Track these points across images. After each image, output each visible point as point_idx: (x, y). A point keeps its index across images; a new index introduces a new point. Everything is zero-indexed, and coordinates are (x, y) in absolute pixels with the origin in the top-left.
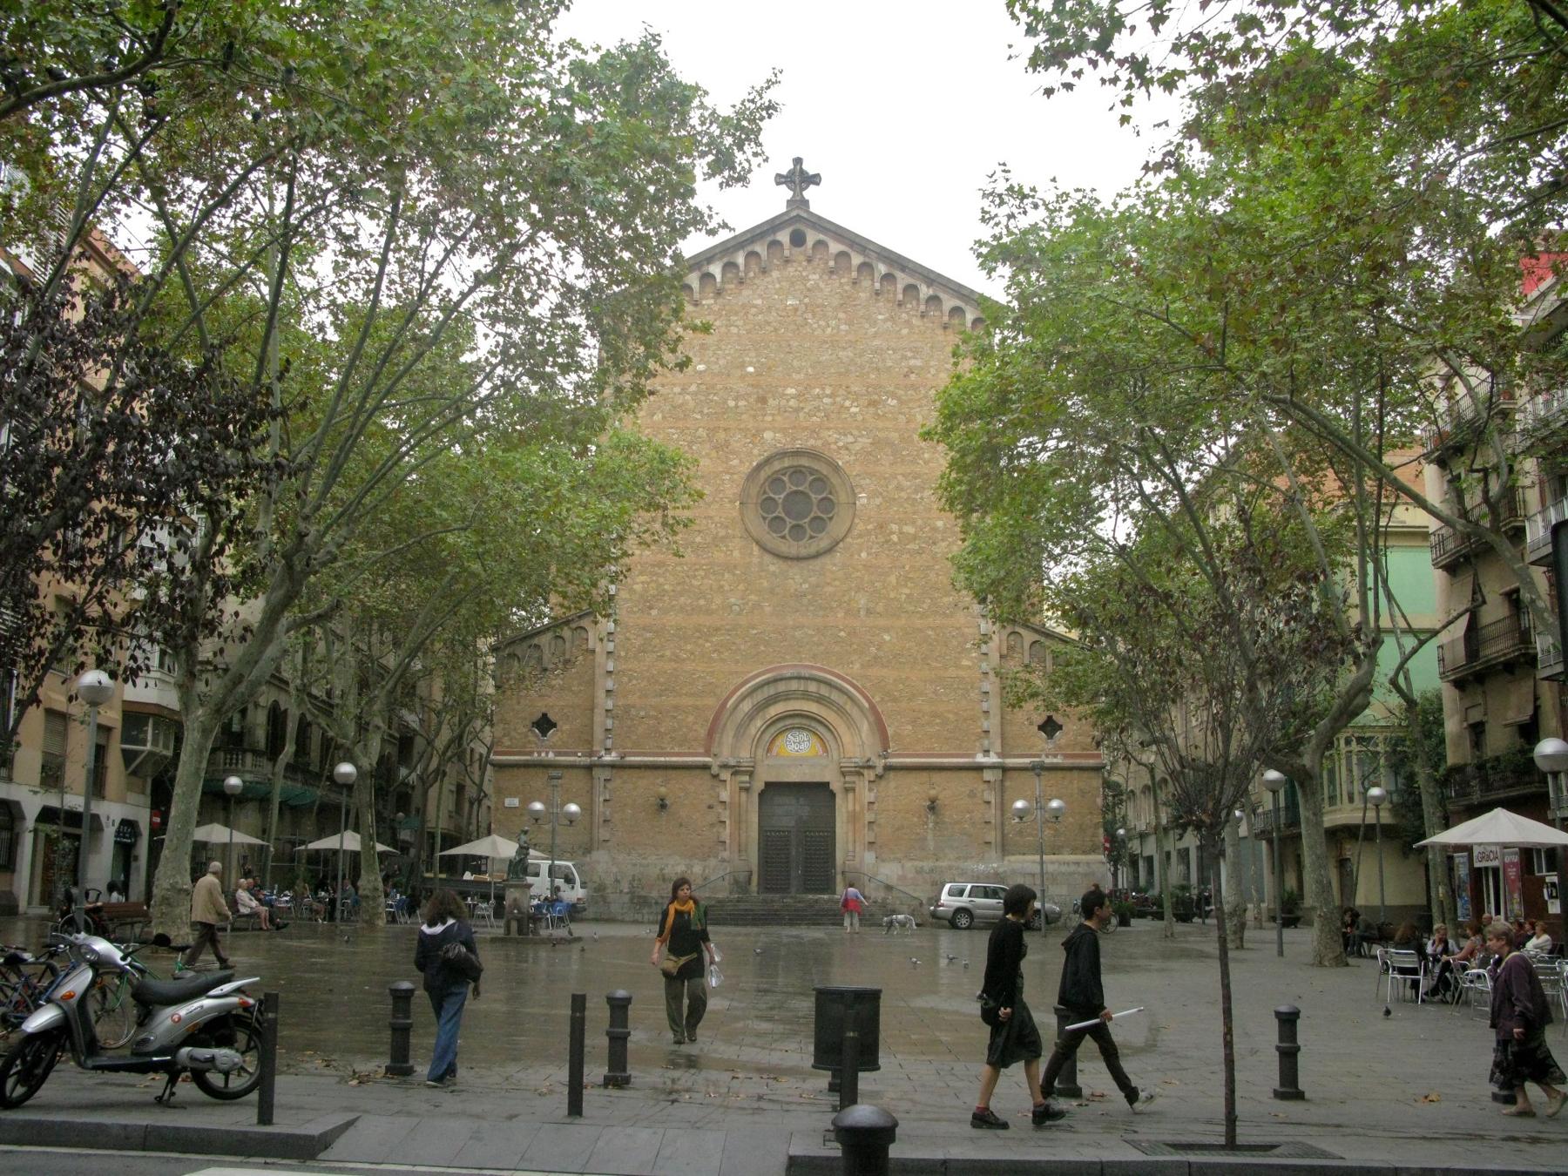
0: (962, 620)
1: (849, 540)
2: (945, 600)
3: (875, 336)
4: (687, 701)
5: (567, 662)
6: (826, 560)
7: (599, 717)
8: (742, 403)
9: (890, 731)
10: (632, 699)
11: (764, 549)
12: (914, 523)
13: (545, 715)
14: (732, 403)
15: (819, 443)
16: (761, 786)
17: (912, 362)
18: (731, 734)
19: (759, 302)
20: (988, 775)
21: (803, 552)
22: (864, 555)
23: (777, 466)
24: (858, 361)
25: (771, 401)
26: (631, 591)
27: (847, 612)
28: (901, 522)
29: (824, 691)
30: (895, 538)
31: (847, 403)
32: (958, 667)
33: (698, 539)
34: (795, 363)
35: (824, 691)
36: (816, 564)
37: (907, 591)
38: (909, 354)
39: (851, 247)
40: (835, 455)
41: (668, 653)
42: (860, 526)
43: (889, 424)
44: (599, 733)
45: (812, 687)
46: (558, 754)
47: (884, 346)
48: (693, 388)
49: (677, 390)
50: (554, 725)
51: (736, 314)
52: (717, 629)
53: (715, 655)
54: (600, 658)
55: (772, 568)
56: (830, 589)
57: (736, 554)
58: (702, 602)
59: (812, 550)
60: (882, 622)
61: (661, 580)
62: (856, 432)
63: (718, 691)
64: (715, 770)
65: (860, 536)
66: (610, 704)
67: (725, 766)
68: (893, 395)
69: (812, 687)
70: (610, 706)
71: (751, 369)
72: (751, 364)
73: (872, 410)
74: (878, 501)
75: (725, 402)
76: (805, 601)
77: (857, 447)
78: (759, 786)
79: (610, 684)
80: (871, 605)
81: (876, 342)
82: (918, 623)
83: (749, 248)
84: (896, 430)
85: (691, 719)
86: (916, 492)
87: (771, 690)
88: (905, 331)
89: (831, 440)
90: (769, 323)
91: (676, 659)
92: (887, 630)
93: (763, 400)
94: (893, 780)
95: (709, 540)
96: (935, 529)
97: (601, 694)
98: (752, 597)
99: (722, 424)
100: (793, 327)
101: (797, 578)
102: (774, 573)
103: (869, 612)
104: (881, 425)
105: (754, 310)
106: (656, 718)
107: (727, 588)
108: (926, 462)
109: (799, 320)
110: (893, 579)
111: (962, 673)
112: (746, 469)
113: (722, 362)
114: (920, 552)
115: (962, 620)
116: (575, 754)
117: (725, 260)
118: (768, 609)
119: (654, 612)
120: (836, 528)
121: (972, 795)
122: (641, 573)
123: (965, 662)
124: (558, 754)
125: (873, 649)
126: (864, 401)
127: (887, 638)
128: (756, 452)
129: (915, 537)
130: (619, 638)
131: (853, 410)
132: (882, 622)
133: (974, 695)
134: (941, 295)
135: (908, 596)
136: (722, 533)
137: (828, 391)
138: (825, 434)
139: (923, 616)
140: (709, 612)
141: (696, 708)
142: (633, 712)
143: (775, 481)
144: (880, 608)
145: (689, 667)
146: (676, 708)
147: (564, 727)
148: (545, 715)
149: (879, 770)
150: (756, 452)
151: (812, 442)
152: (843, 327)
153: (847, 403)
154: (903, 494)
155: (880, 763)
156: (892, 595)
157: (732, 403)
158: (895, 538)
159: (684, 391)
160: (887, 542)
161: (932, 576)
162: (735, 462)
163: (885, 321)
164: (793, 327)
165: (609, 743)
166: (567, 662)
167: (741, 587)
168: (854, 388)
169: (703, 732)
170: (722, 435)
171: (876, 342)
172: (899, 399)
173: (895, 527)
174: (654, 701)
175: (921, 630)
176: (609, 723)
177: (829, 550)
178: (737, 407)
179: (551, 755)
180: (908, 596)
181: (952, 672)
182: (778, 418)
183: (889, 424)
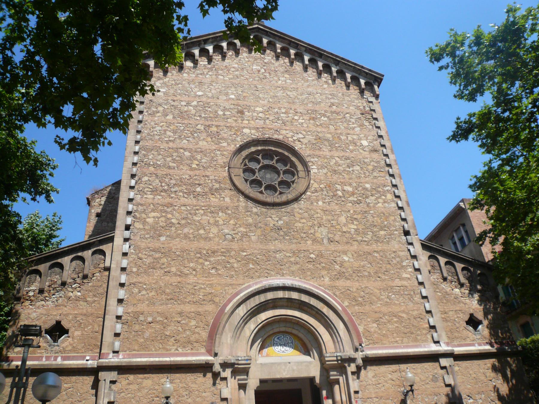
0: (397, 246)
1: (308, 193)
2: (382, 233)
3: (308, 86)
4: (188, 308)
5: (85, 277)
6: (295, 205)
7: (110, 320)
8: (227, 113)
9: (361, 329)
10: (142, 307)
11: (247, 197)
12: (350, 185)
13: (58, 323)
14: (221, 113)
15: (281, 137)
16: (258, 384)
17: (332, 101)
18: (230, 335)
19: (236, 66)
20: (444, 362)
21: (277, 200)
22: (320, 203)
23: (253, 149)
24: (299, 97)
25: (246, 113)
26: (144, 223)
27: (315, 241)
28: (343, 184)
29: (305, 298)
30: (340, 193)
31: (296, 118)
32: (401, 279)
33: (199, 189)
34: (261, 95)
35: (305, 298)
36: (289, 208)
37: (355, 227)
38: (330, 97)
39: (289, 45)
40: (292, 144)
41: (174, 269)
42: (316, 185)
43: (323, 130)
44: (108, 336)
45: (295, 295)
46: (64, 358)
47: (315, 92)
48: (195, 103)
49: (184, 103)
50: (66, 332)
51: (222, 70)
52: (214, 252)
53: (213, 271)
54: (115, 272)
55: (255, 210)
56: (299, 225)
57: (227, 199)
58: (202, 232)
59: (284, 198)
60: (340, 248)
61: (169, 216)
62: (304, 133)
63: (217, 300)
64: (217, 368)
65: (316, 191)
66: (120, 311)
67: (225, 365)
68: (325, 116)
69: (295, 295)
70: (120, 314)
71: (233, 97)
72: (232, 94)
73: (312, 122)
74: (325, 171)
75: (216, 112)
76: (282, 233)
77: (305, 141)
78: (253, 383)
79: (122, 293)
80: (330, 235)
81: (310, 89)
82: (367, 248)
83: (230, 40)
84: (330, 133)
85: (193, 323)
86: (349, 167)
87: (262, 298)
88: (325, 86)
89: (288, 136)
90: (243, 76)
91: (181, 274)
92: (345, 253)
93: (242, 112)
94: (370, 372)
95: (206, 190)
96: (365, 189)
97: (112, 302)
98: (242, 229)
99: (214, 123)
100: (257, 79)
101: (274, 217)
102: (256, 214)
103: (330, 241)
104: (319, 129)
105: (233, 69)
106: (162, 323)
107: (221, 222)
108: (352, 151)
109: (262, 76)
110: (343, 219)
111: (405, 283)
112: (233, 148)
113: (213, 91)
114: (359, 202)
115: (397, 246)
116: (83, 358)
117: (215, 43)
118: (253, 238)
119: (163, 239)
120: (299, 186)
121: (435, 379)
122: (153, 211)
123: (405, 275)
124: (64, 358)
125: (337, 267)
126: (307, 117)
127: (346, 259)
128: (238, 139)
129: (353, 194)
130: (132, 257)
131: (300, 121)
132: (340, 248)
133: (418, 298)
134: (345, 70)
135: (356, 230)
136: (217, 186)
137: (283, 110)
138: (284, 132)
139: (368, 243)
140: (207, 239)
141: (199, 314)
142: (141, 318)
143: (252, 158)
144: (337, 238)
145: (192, 279)
146: (180, 314)
147: (75, 333)
148: (58, 323)
149: (360, 362)
150: (238, 139)
151: (276, 136)
152: (288, 81)
153: (296, 118)
154: (340, 167)
155: (359, 356)
156: (345, 229)
157: (221, 113)
158: (340, 193)
159: (188, 104)
160: (335, 195)
161: (369, 217)
162: (225, 144)
163: (313, 80)
164: (257, 79)
165: (117, 345)
166: (85, 277)
167: (232, 222)
168: (299, 110)
169: (205, 335)
170: (214, 129)
171: (310, 89)
172: (328, 117)
173: (339, 187)
174: (160, 309)
175: (369, 254)
176: (119, 328)
177: (296, 199)
178: (224, 115)
179: (59, 359)
180: (356, 230)
181: (397, 282)
182: (252, 122)
183: (323, 130)
